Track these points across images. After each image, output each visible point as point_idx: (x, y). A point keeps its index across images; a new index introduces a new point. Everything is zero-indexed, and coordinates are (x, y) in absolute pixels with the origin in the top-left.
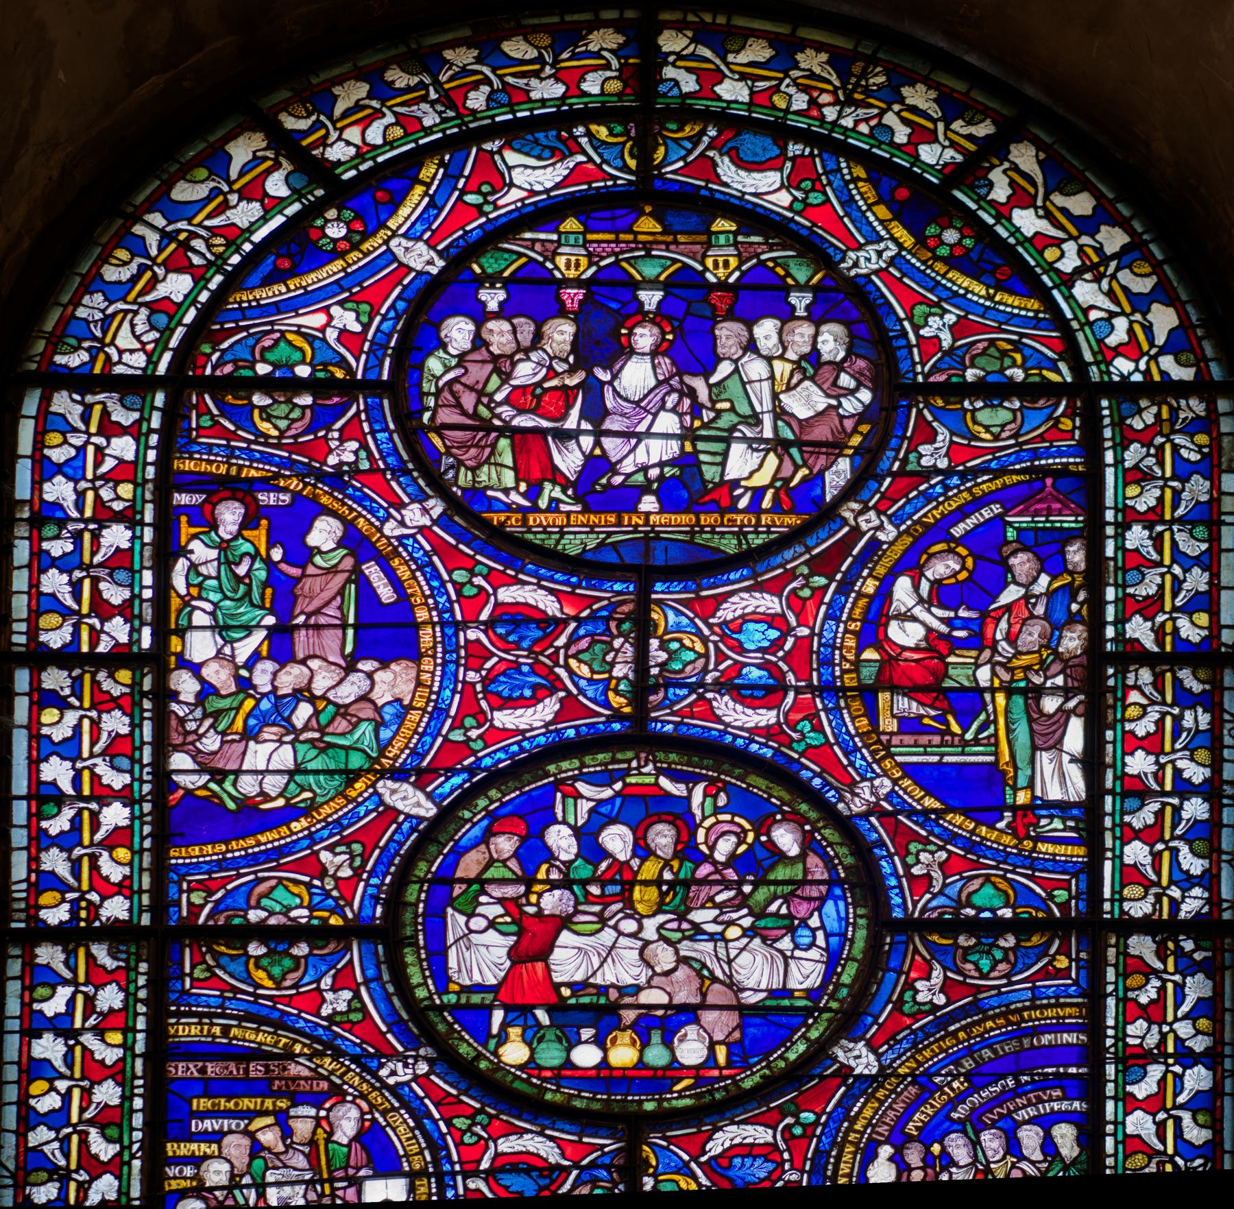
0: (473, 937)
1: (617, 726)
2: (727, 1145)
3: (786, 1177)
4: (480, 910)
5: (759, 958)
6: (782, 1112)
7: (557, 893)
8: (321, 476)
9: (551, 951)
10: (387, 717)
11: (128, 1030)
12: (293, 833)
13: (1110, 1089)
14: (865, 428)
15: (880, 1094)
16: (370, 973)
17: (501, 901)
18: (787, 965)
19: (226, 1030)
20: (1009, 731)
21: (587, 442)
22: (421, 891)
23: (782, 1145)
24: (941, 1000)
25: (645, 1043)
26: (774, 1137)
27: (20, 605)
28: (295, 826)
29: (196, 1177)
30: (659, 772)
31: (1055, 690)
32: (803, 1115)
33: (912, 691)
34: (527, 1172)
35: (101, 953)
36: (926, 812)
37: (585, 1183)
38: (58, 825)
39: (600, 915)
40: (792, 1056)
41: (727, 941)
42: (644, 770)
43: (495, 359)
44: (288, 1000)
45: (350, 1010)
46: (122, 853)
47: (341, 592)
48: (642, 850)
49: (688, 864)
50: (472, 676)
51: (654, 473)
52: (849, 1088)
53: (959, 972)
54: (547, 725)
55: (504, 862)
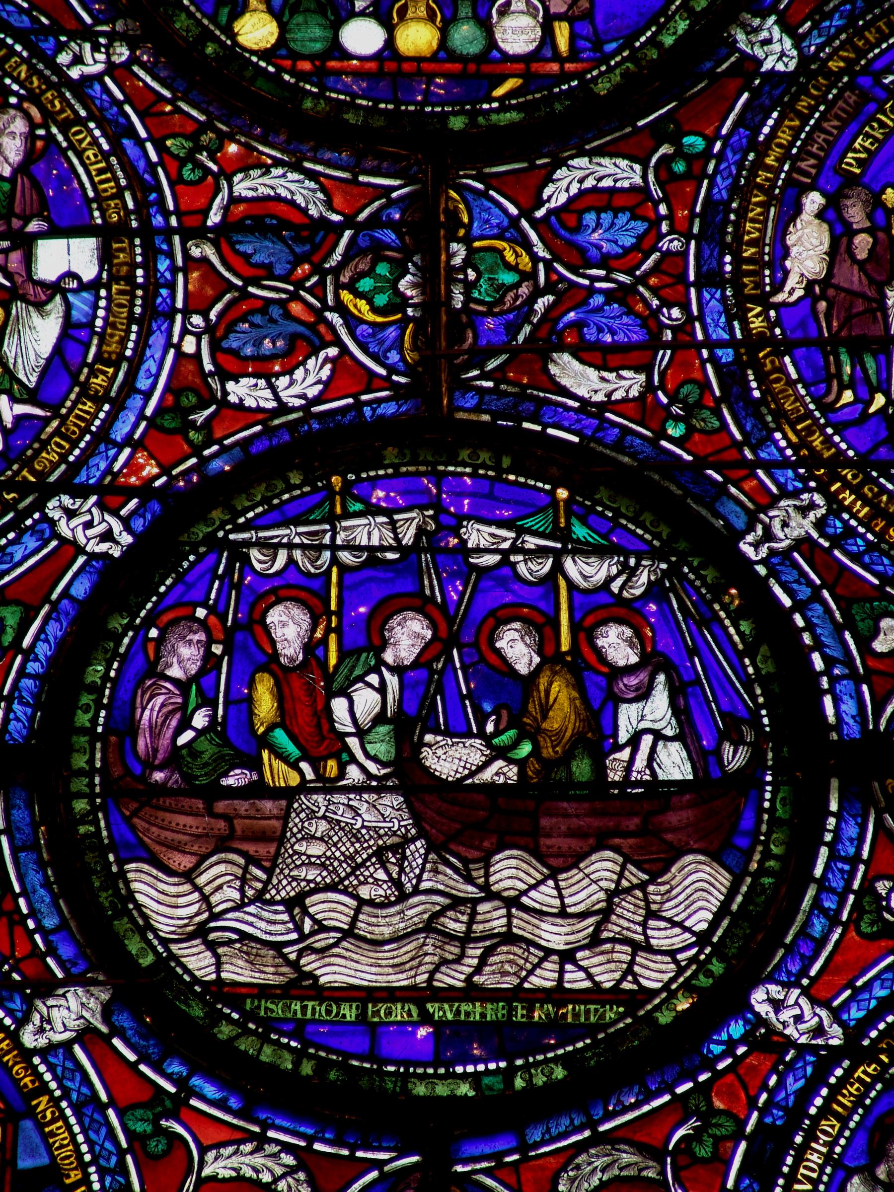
2: (574, 190)
3: (664, 245)
15: (803, 104)
23: (656, 191)
26: (644, 177)
32: (688, 140)
37: (363, 252)
40: (668, 40)
52: (755, 94)
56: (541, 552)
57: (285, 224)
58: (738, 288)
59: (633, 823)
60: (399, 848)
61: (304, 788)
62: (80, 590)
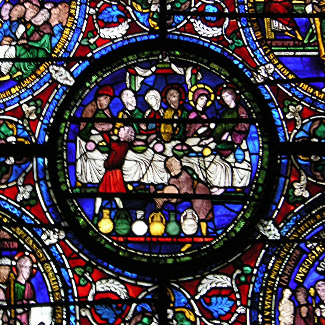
0: (89, 154)
4: (92, 138)
5: (219, 167)
7: (127, 128)
9: (123, 163)
10: (56, 32)
12: (12, 94)
18: (232, 171)
22: (66, 127)
28: (13, 90)
30: (172, 61)
41: (204, 157)
42: (165, 60)
48: (165, 103)
49: (186, 113)
54: (123, 36)
55: (103, 110)
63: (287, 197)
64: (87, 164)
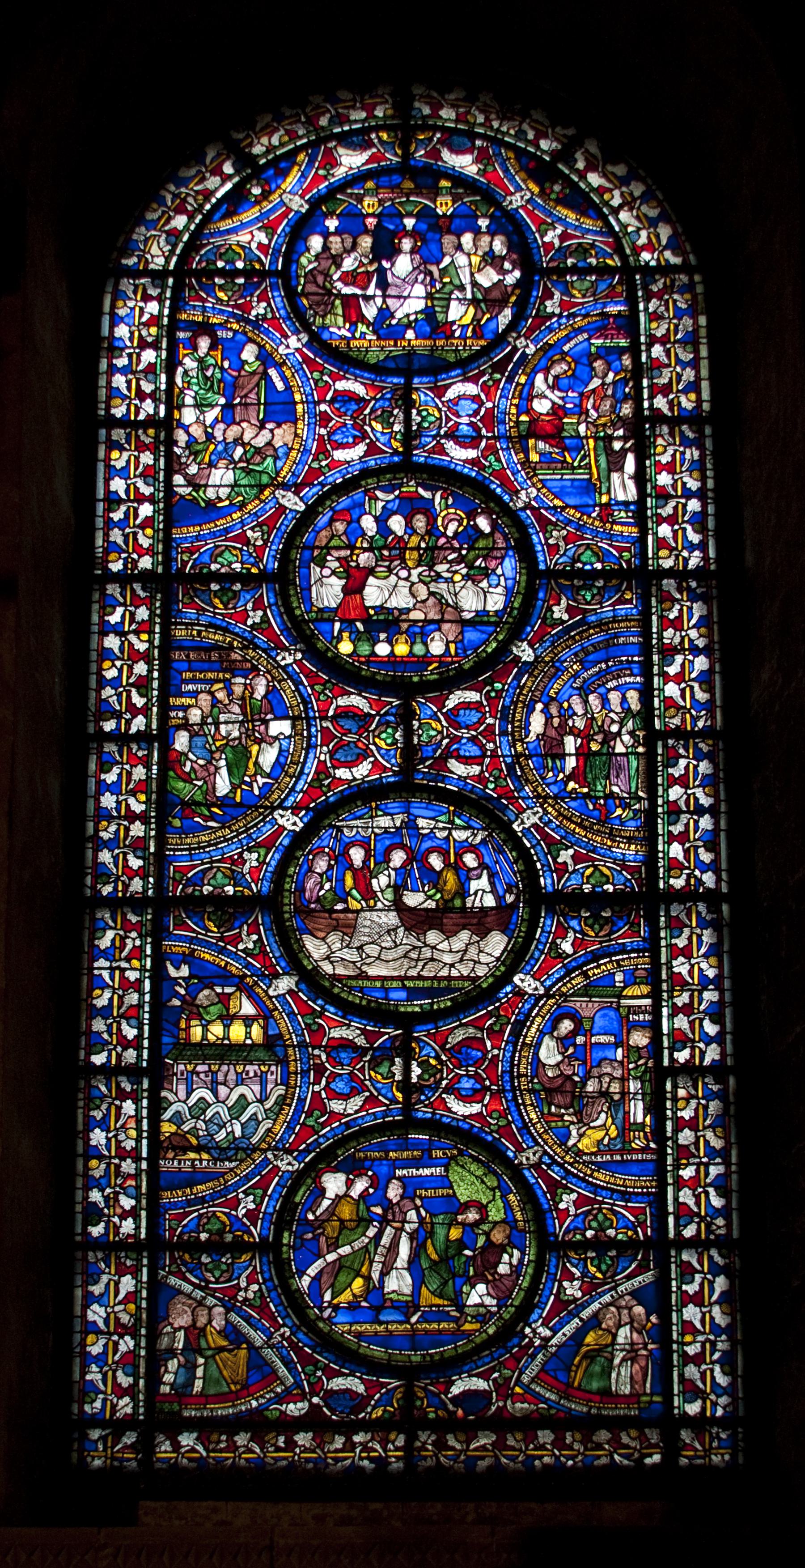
1: (396, 459)
6: (485, 683)
8: (248, 321)
11: (151, 632)
13: (656, 669)
14: (517, 292)
16: (272, 601)
17: (338, 559)
19: (199, 632)
20: (596, 461)
21: (379, 301)
24: (565, 617)
25: (413, 644)
27: (102, 393)
28: (235, 516)
29: (186, 718)
30: (418, 485)
31: (618, 438)
33: (545, 438)
34: (353, 718)
35: (137, 587)
36: (555, 507)
38: (117, 516)
39: (388, 567)
40: (489, 650)
43: (334, 257)
44: (231, 616)
45: (262, 621)
46: (149, 531)
47: (258, 385)
50: (323, 431)
51: (412, 318)
53: (575, 601)
56: (444, 828)
57: (355, 715)
58: (513, 736)
59: (475, 921)
60: (395, 930)
61: (362, 910)
62: (286, 842)
63: (544, 619)
64: (323, 590)
